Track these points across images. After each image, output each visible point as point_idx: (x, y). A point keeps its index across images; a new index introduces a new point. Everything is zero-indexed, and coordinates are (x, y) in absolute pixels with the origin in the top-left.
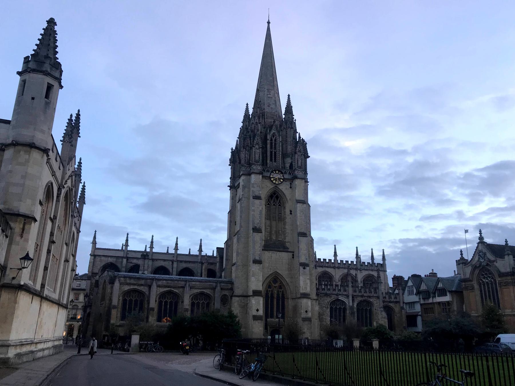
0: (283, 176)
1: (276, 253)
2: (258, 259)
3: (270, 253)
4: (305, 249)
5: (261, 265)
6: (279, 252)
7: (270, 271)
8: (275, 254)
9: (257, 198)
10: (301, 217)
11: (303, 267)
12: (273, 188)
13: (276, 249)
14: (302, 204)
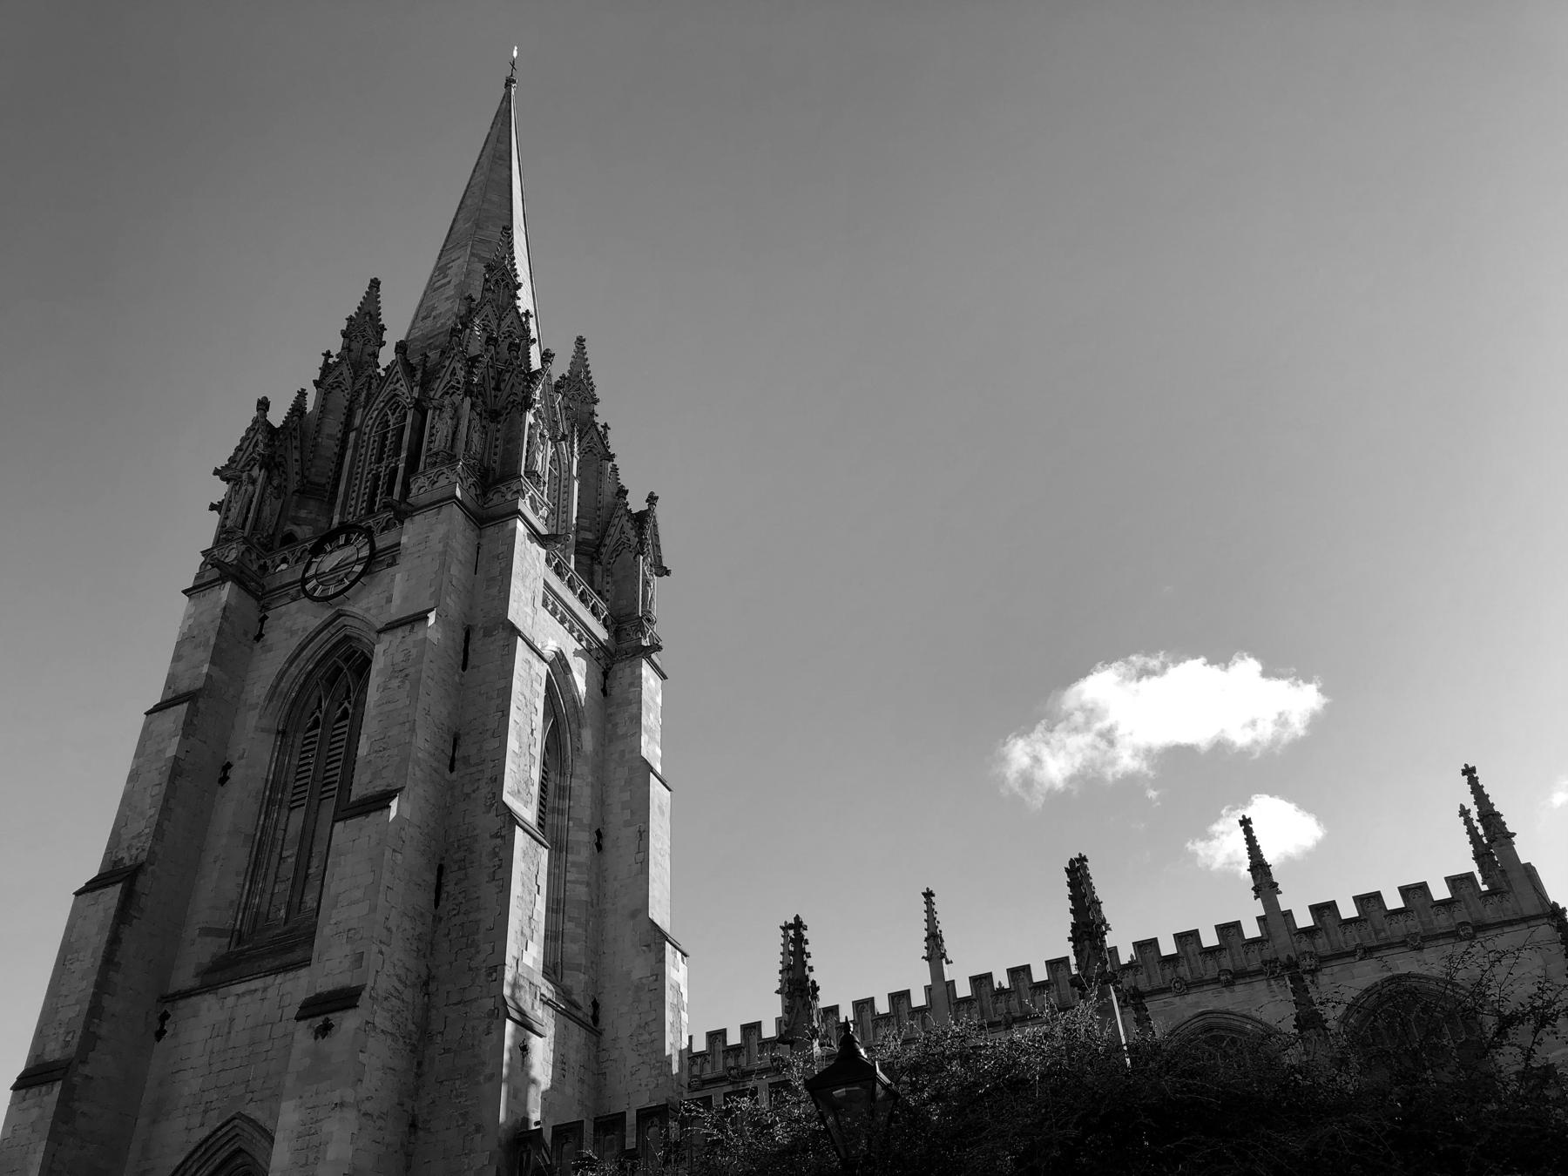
0: (373, 547)
1: (265, 990)
2: (57, 1055)
3: (231, 1001)
4: (358, 894)
5: (58, 1087)
6: (280, 979)
7: (202, 1125)
8: (259, 995)
9: (176, 701)
10: (391, 707)
11: (319, 1021)
12: (326, 625)
13: (269, 963)
14: (408, 627)
